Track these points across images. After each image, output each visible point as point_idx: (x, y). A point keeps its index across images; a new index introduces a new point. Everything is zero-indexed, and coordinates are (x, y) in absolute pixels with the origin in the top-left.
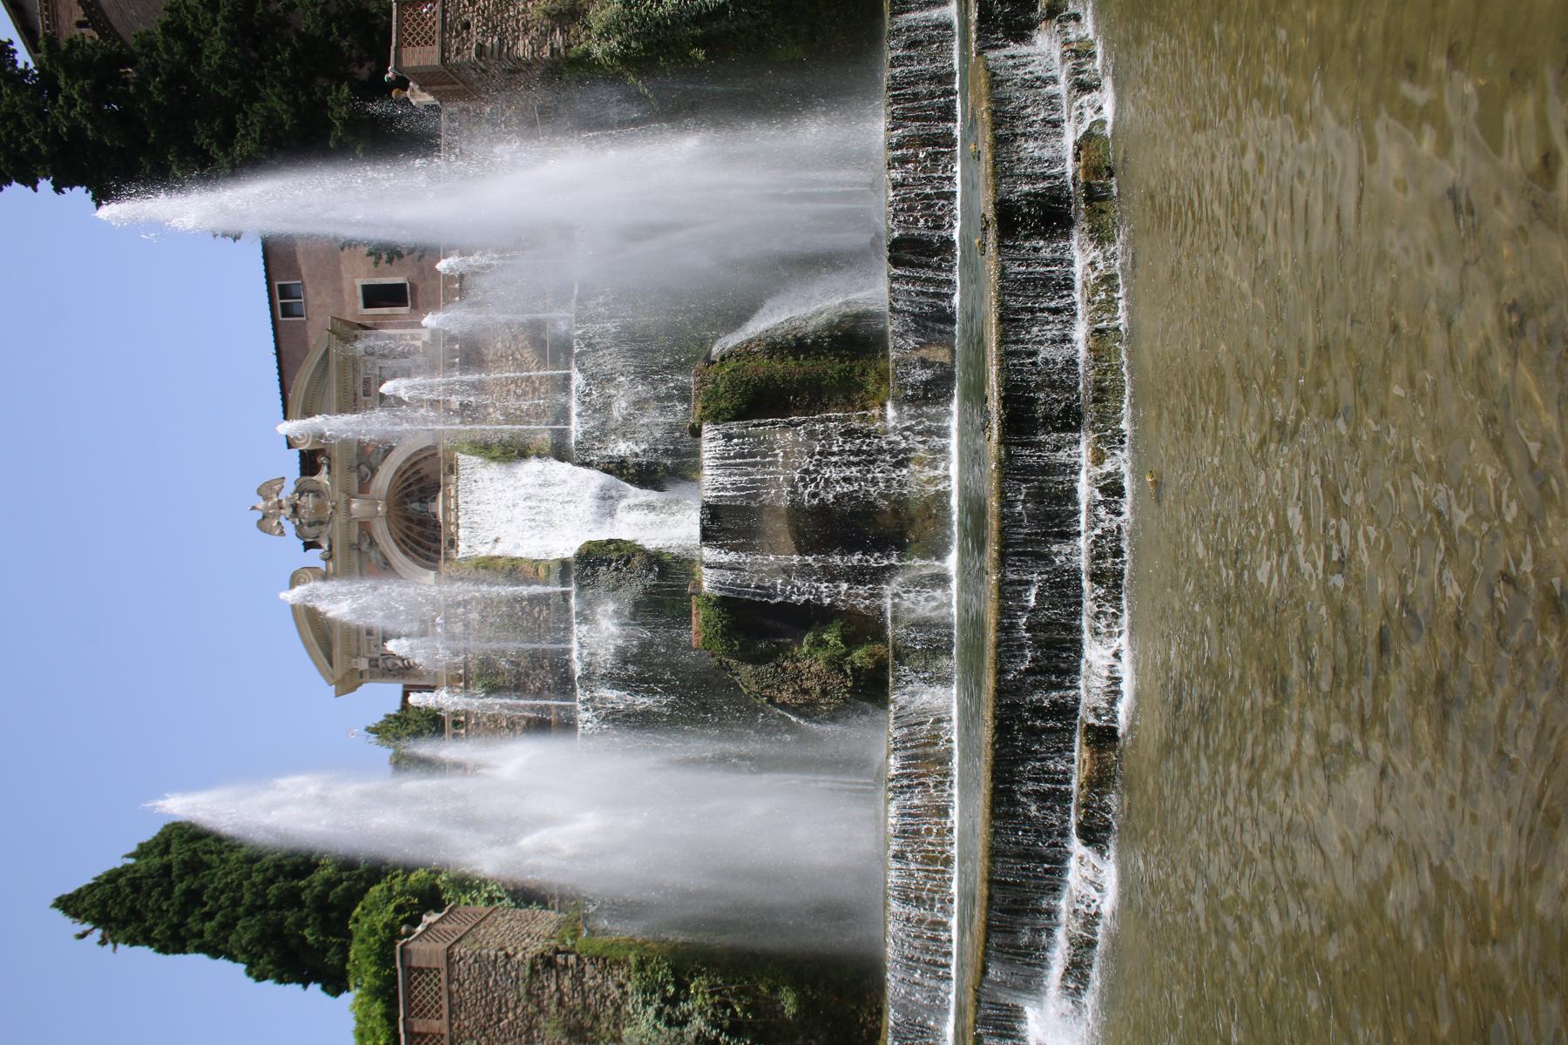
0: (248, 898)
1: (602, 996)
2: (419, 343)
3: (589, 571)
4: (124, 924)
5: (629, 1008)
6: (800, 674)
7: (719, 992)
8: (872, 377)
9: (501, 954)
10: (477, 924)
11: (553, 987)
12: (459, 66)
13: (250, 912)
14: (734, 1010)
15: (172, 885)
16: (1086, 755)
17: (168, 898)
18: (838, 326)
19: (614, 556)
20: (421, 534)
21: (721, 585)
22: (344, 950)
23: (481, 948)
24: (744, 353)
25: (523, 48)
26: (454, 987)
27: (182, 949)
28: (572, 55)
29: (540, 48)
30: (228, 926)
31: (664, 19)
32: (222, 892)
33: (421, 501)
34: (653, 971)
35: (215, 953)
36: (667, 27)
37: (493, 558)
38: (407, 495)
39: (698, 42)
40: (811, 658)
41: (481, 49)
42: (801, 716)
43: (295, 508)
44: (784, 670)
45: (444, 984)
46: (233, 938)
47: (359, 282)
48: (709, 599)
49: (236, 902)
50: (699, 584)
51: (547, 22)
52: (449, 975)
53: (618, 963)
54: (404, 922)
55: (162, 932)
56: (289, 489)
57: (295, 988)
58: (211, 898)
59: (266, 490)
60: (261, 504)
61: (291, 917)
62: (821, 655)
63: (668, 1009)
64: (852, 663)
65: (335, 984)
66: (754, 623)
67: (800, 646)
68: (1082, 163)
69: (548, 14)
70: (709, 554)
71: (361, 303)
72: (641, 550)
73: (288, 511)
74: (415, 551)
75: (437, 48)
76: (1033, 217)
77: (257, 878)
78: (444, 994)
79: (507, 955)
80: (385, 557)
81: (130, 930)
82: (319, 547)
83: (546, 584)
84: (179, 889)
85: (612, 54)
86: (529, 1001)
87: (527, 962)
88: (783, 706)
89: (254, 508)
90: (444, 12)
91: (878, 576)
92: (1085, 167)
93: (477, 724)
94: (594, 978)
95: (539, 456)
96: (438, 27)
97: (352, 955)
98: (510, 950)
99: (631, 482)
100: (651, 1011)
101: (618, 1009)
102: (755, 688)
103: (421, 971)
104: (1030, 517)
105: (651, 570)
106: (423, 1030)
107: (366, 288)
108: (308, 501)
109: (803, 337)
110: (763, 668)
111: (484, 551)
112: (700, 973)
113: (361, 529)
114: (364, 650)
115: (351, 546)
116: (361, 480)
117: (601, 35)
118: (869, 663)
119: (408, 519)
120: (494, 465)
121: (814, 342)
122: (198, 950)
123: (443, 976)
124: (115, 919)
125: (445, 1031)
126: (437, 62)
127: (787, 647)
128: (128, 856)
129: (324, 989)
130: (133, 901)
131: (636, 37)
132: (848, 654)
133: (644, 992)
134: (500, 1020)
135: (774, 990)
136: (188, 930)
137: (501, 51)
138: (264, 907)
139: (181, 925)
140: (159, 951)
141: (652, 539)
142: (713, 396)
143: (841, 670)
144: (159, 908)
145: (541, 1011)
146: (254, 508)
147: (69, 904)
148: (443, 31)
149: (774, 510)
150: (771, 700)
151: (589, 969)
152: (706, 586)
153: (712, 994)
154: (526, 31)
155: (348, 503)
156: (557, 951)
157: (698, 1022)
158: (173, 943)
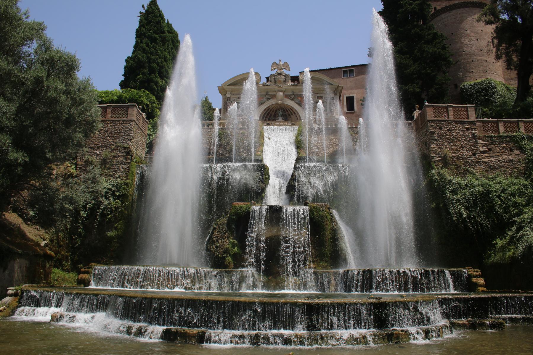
0: (153, 57)
1: (116, 171)
2: (335, 114)
3: (259, 169)
4: (146, 19)
5: (112, 180)
7: (116, 210)
8: (324, 264)
10: (142, 130)
11: (120, 155)
12: (427, 126)
13: (148, 58)
14: (109, 214)
15: (158, 34)
16: (195, 332)
17: (154, 33)
18: (342, 253)
19: (264, 177)
20: (271, 115)
21: (254, 212)
22: (135, 88)
24: (333, 220)
25: (434, 147)
26: (121, 122)
27: (137, 37)
28: (432, 163)
29: (434, 152)
30: (144, 51)
31: (445, 194)
32: (155, 49)
33: (282, 115)
34: (124, 188)
35: (135, 47)
36: (442, 195)
37: (263, 137)
38: (284, 110)
39: (438, 205)
40: (228, 242)
41: (433, 133)
42: (209, 239)
43: (280, 74)
44: (225, 233)
45: (122, 119)
46: (140, 52)
47: (355, 95)
48: (249, 208)
49: (151, 53)
50: (255, 205)
51: (443, 155)
52: (125, 120)
53: (127, 176)
54: (143, 107)
55: (143, 31)
56: (287, 72)
57: (123, 72)
58: (153, 46)
59: (286, 65)
60: (281, 63)
61: (146, 71)
63: (111, 192)
64: (227, 257)
65: (123, 85)
66: (241, 223)
68: (400, 332)
69: (445, 155)
70: (264, 208)
71: (348, 96)
72: (266, 186)
73: (279, 72)
74: (265, 113)
75: (433, 119)
76: (381, 315)
77: (159, 60)
78: (119, 119)
79: (131, 139)
80: (264, 103)
81: (144, 21)
82: (267, 82)
83: (255, 155)
85: (433, 176)
86: (116, 147)
87: (128, 146)
88: (213, 233)
90: (445, 121)
92: (399, 333)
94: (122, 168)
95: (298, 153)
96: (440, 119)
97: (132, 90)
98: (133, 140)
99: (289, 183)
100: (110, 187)
101: (111, 176)
102: (219, 223)
103: (127, 111)
104: (277, 313)
105: (259, 189)
106: (108, 112)
107: (353, 97)
108: (282, 78)
109: (338, 241)
110: (225, 226)
111: (266, 134)
112: (122, 203)
113: (273, 95)
114: (233, 96)
115: (267, 92)
116: (289, 96)
117: (439, 173)
118: (227, 262)
119: (276, 111)
120: (294, 138)
121: (336, 244)
122: (137, 42)
123: (125, 118)
124: (148, 16)
125: (107, 119)
126: (428, 119)
127: (232, 235)
129: (122, 81)
130: (153, 22)
131: (439, 184)
132: (230, 255)
133: (117, 185)
134: (110, 137)
135: (116, 228)
137: (433, 140)
138: (149, 62)
139: (145, 37)
140: (137, 29)
141: (269, 190)
142: (318, 210)
143: (225, 253)
144: (151, 30)
145: (112, 150)
148: (439, 121)
149: (279, 230)
150: (215, 229)
151: (125, 166)
153: (115, 207)
154: (439, 148)
155: (282, 91)
156: (132, 156)
157: (106, 203)
158: (139, 34)
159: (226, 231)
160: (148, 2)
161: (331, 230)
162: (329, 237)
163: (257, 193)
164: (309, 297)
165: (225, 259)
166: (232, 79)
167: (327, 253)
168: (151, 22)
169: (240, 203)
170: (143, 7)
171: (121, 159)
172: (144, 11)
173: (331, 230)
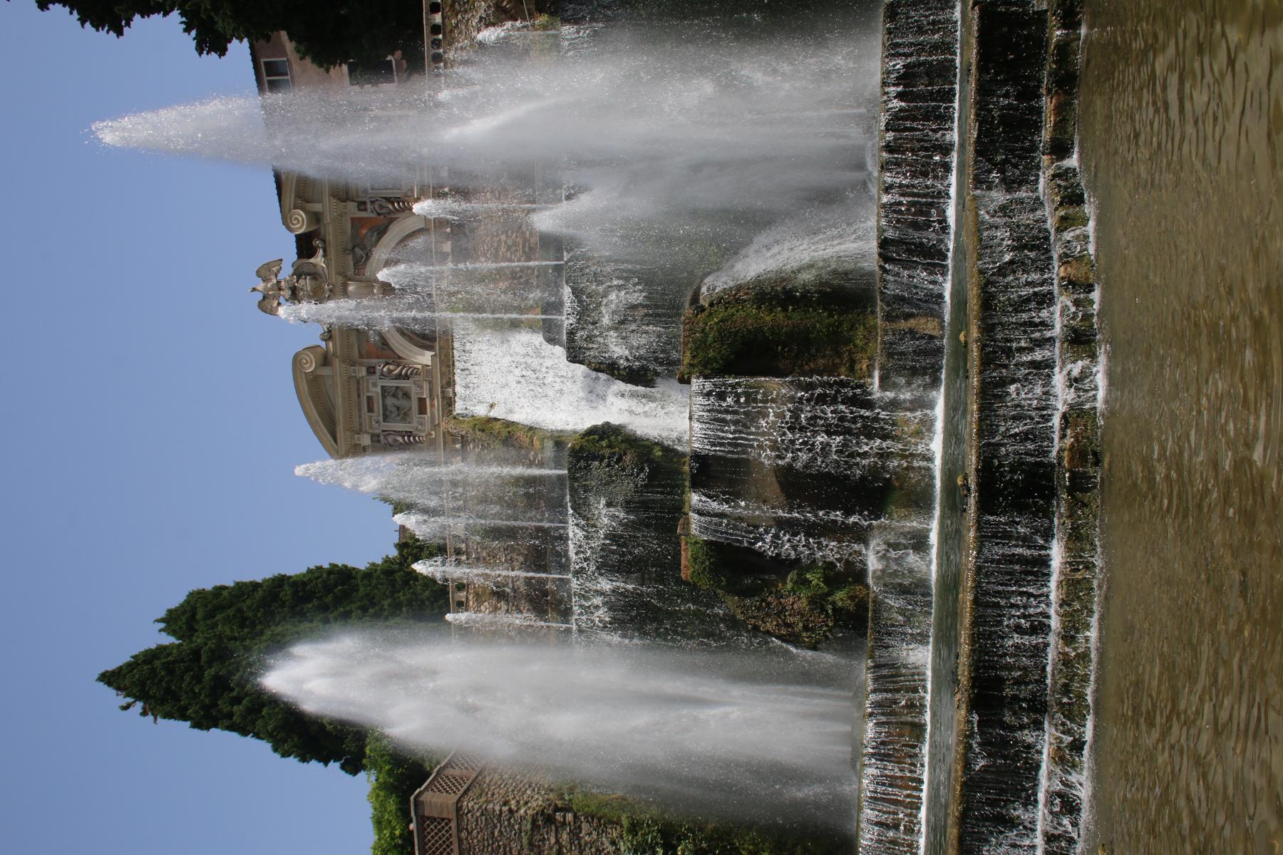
1: (597, 850)
3: (582, 463)
4: (162, 701)
6: (784, 609)
8: (860, 332)
9: (505, 809)
11: (553, 840)
15: (202, 670)
19: (607, 452)
23: (487, 802)
24: (732, 299)
26: (464, 834)
44: (769, 604)
45: (454, 831)
52: (458, 825)
55: (196, 712)
56: (286, 272)
59: (265, 272)
60: (261, 286)
62: (804, 594)
64: (833, 603)
67: (785, 583)
73: (287, 293)
78: (454, 839)
79: (510, 811)
83: (541, 465)
84: (209, 673)
86: (532, 850)
87: (530, 819)
89: (254, 289)
91: (861, 535)
93: (478, 559)
94: (590, 834)
103: (433, 819)
109: (791, 291)
110: (748, 602)
111: (481, 411)
121: (803, 296)
123: (453, 824)
128: (158, 621)
132: (830, 594)
136: (219, 711)
139: (214, 705)
140: (194, 726)
142: (700, 346)
143: (823, 610)
146: (254, 289)
147: (109, 678)
151: (585, 826)
152: (694, 529)
156: (557, 809)
158: (204, 721)
159: (763, 601)
160: (111, 692)
161: (759, 308)
162: (781, 316)
163: (650, 477)
164: (954, 409)
165: (841, 609)
166: (315, 432)
167: (830, 325)
168: (168, 691)
169: (683, 562)
170: (126, 708)
171: (565, 836)
172: (139, 706)
173: (759, 308)
